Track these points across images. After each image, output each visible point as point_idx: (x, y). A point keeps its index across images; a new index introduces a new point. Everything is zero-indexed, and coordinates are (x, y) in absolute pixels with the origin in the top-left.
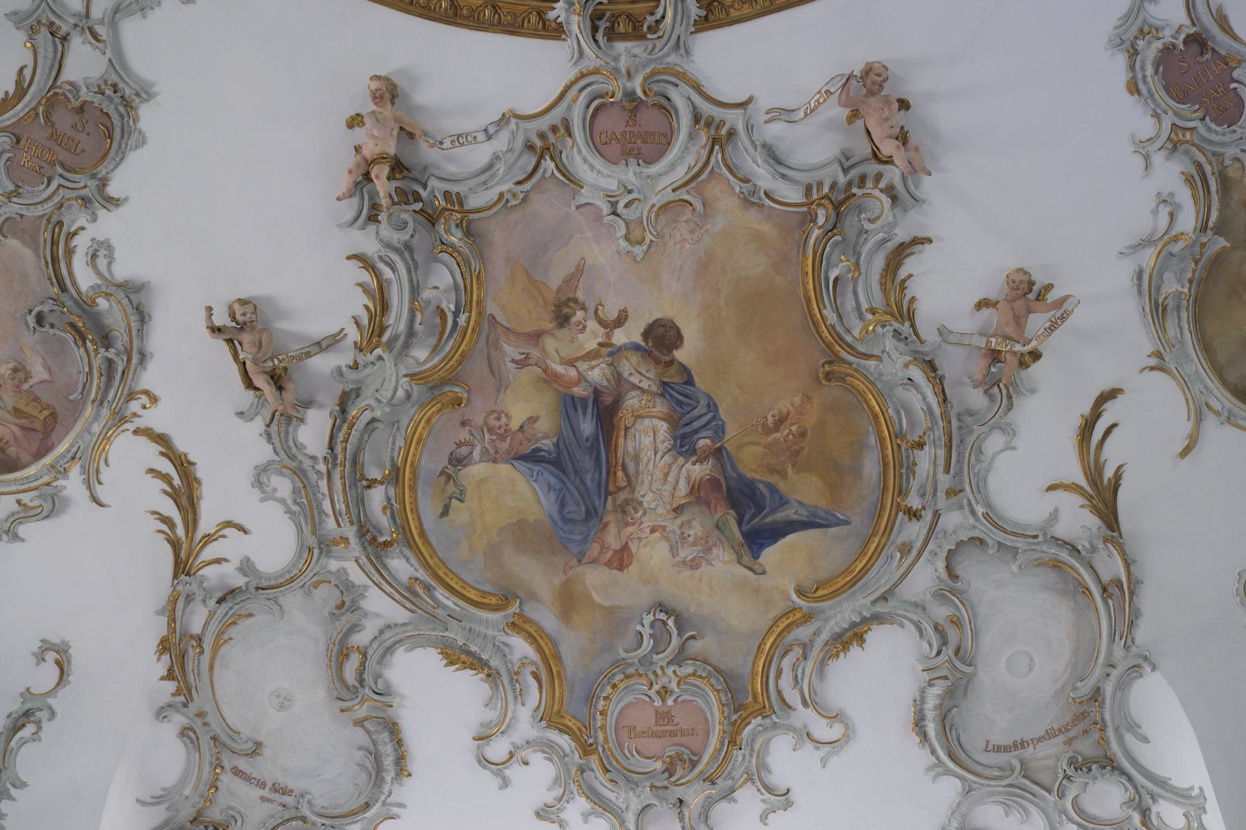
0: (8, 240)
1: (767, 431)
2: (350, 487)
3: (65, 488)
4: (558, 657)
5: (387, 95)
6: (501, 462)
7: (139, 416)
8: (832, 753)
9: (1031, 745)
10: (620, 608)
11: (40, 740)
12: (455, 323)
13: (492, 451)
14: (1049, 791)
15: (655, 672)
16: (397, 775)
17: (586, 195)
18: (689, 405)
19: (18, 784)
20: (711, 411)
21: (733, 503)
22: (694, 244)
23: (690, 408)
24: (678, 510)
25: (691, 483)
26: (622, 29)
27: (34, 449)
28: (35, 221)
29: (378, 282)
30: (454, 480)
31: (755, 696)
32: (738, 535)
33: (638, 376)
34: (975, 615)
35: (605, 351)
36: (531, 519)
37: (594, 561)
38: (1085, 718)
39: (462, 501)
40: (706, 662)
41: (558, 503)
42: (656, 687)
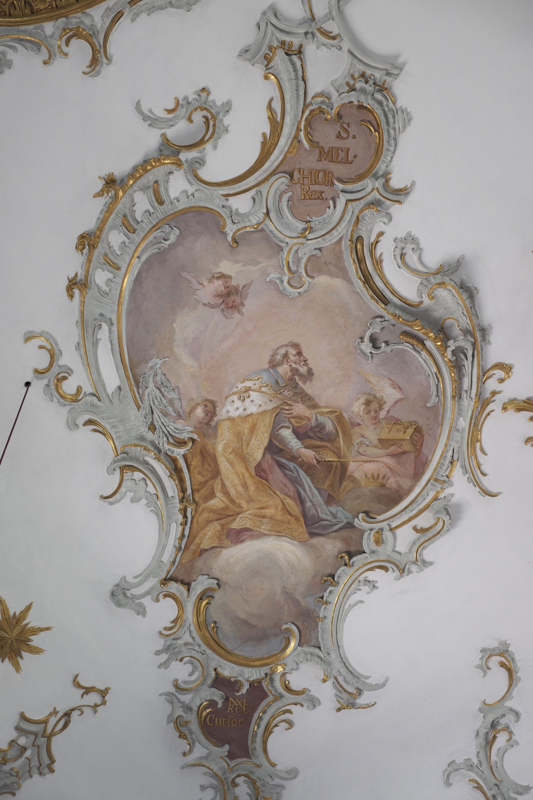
0: (316, 280)
3: (452, 495)
7: (499, 392)
11: (517, 743)
19: (520, 790)
27: (411, 471)
28: (334, 249)
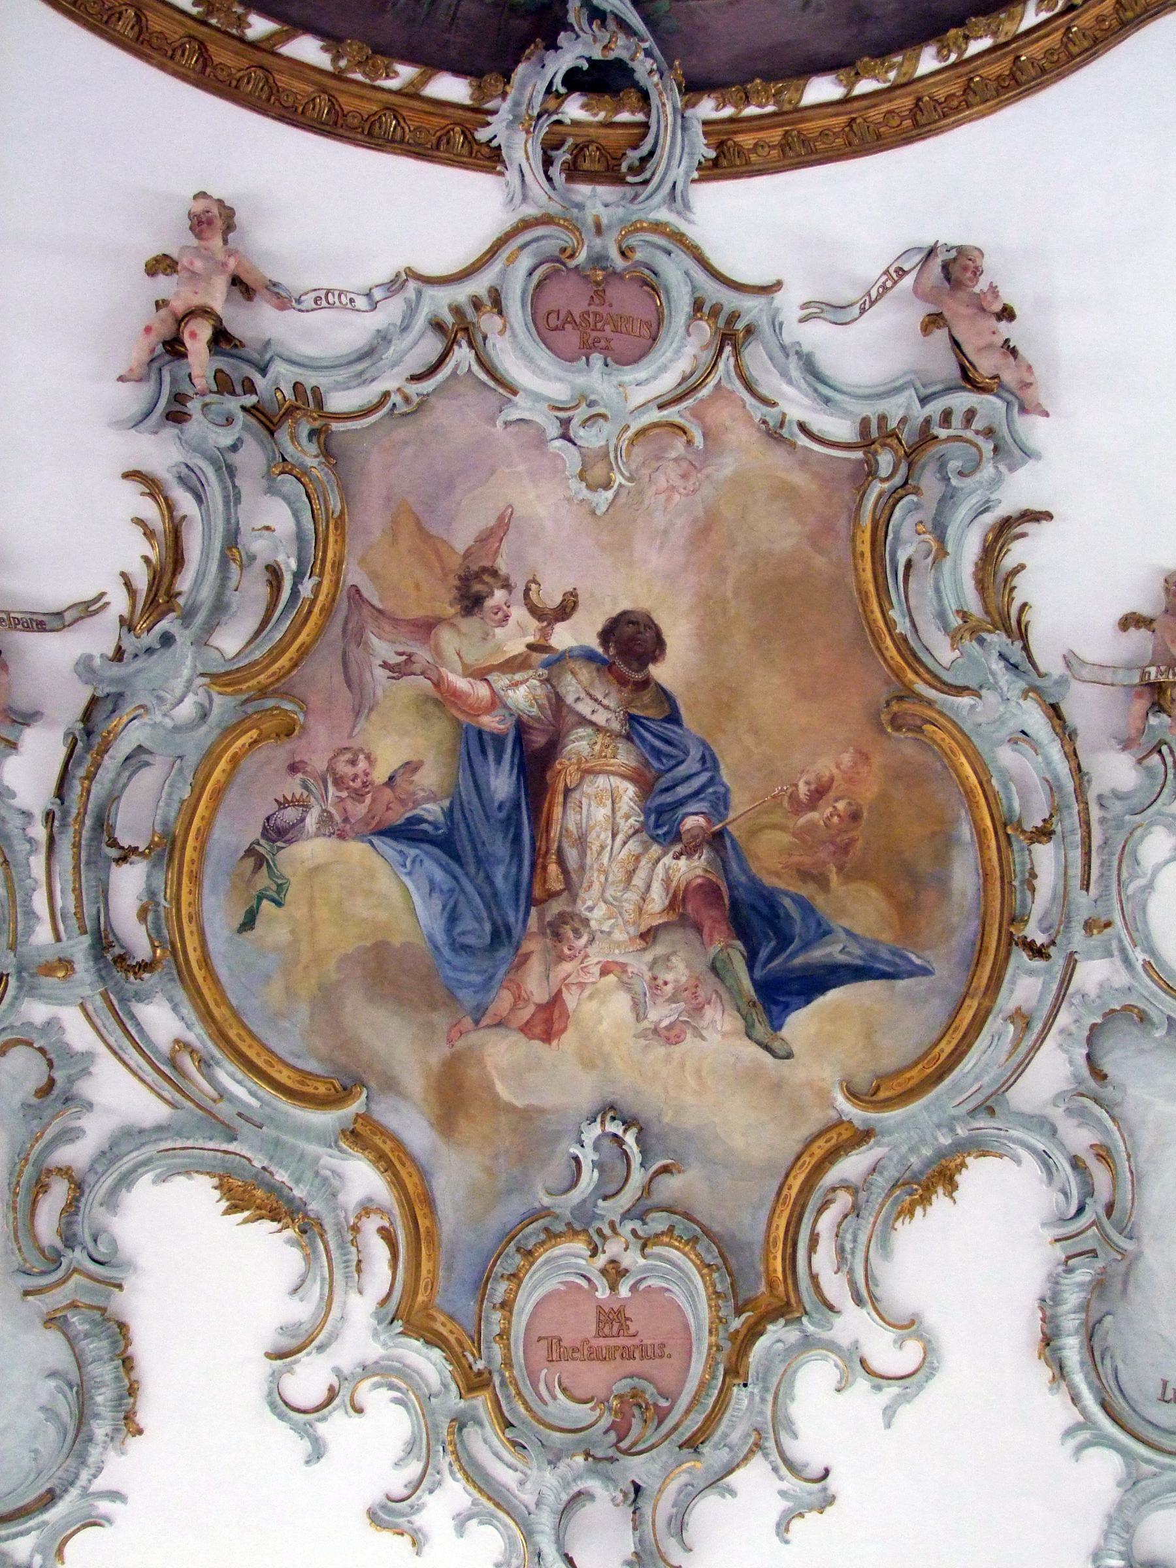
1: (798, 807)
2: (87, 863)
4: (429, 1201)
5: (219, 223)
6: (354, 839)
8: (904, 1398)
10: (541, 1111)
12: (295, 593)
13: (338, 818)
15: (599, 1232)
16: (117, 1430)
17: (521, 408)
18: (670, 756)
20: (706, 770)
21: (742, 930)
22: (687, 495)
23: (673, 762)
24: (648, 936)
25: (672, 891)
26: (587, 165)
29: (171, 517)
30: (269, 866)
31: (771, 1285)
32: (747, 984)
33: (590, 702)
35: (538, 658)
36: (397, 941)
37: (500, 1024)
39: (279, 904)
40: (687, 1216)
41: (446, 915)
42: (601, 1260)
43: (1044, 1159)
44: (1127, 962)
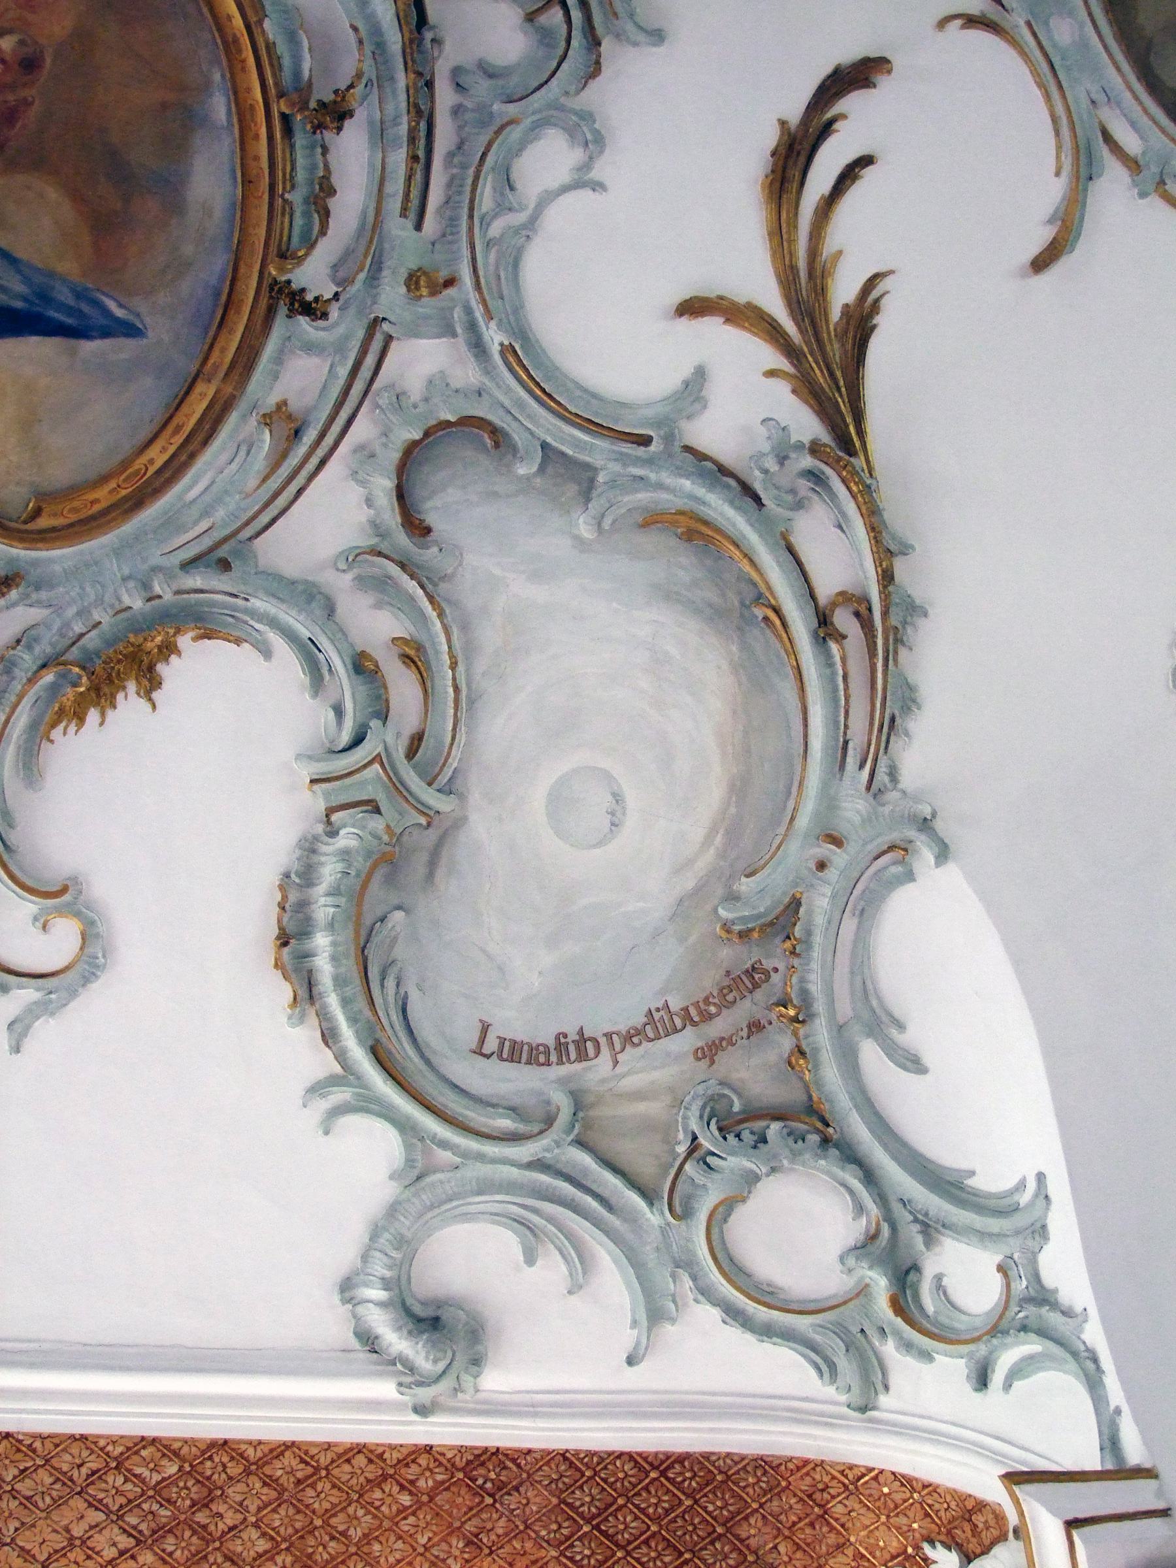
9: (605, 1050)
14: (649, 1196)
34: (471, 648)
38: (756, 986)
43: (309, 652)
44: (478, 347)
